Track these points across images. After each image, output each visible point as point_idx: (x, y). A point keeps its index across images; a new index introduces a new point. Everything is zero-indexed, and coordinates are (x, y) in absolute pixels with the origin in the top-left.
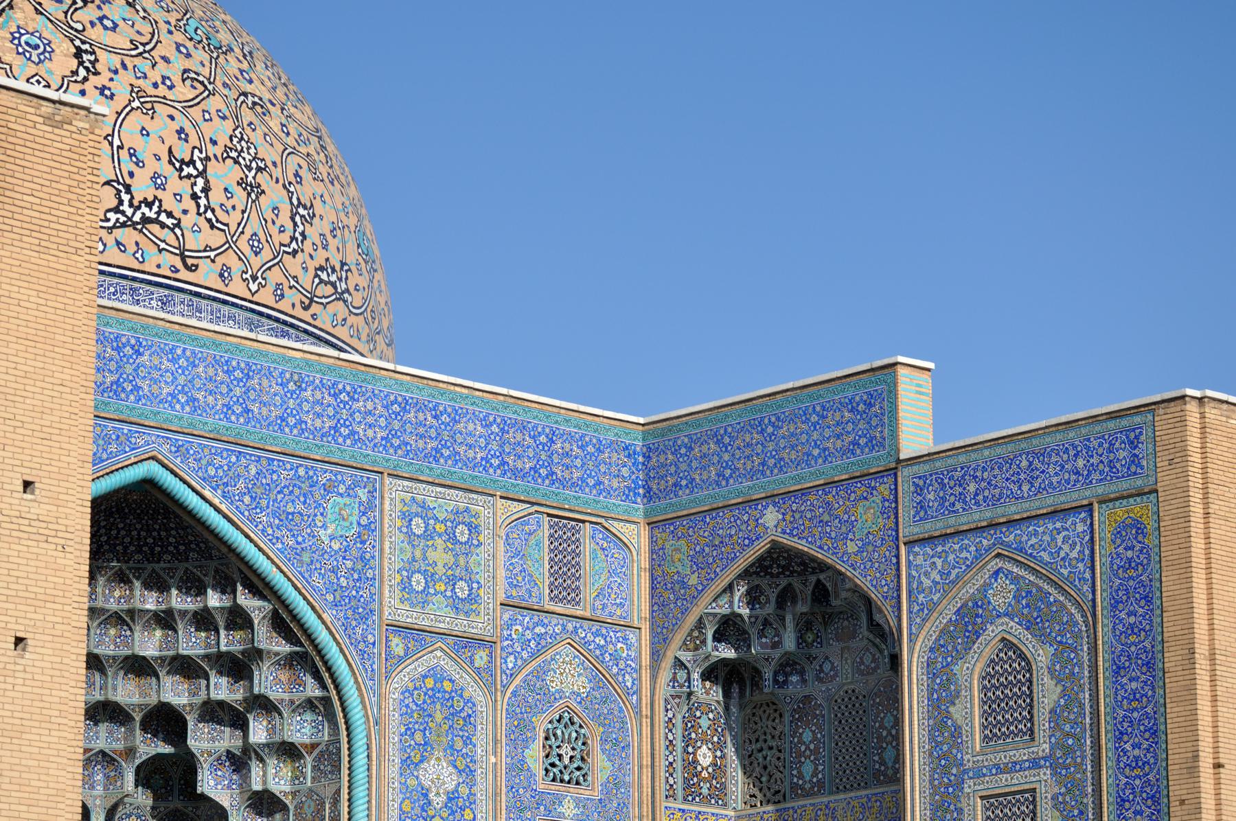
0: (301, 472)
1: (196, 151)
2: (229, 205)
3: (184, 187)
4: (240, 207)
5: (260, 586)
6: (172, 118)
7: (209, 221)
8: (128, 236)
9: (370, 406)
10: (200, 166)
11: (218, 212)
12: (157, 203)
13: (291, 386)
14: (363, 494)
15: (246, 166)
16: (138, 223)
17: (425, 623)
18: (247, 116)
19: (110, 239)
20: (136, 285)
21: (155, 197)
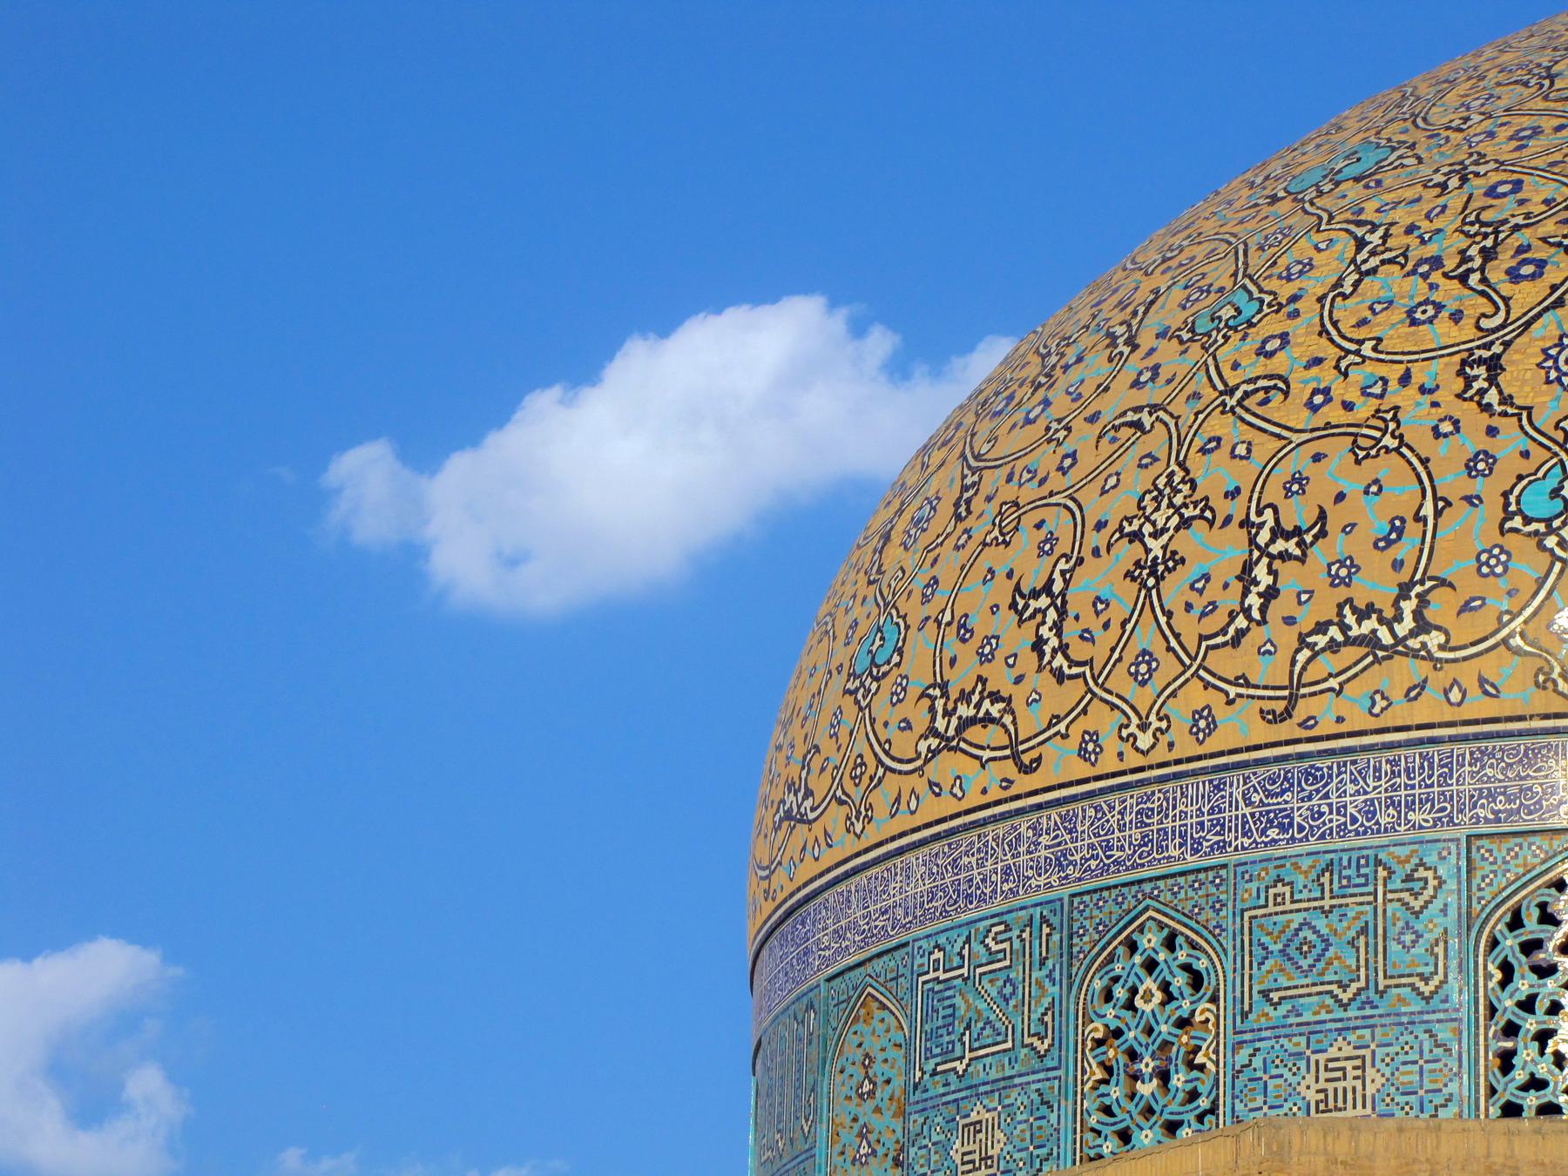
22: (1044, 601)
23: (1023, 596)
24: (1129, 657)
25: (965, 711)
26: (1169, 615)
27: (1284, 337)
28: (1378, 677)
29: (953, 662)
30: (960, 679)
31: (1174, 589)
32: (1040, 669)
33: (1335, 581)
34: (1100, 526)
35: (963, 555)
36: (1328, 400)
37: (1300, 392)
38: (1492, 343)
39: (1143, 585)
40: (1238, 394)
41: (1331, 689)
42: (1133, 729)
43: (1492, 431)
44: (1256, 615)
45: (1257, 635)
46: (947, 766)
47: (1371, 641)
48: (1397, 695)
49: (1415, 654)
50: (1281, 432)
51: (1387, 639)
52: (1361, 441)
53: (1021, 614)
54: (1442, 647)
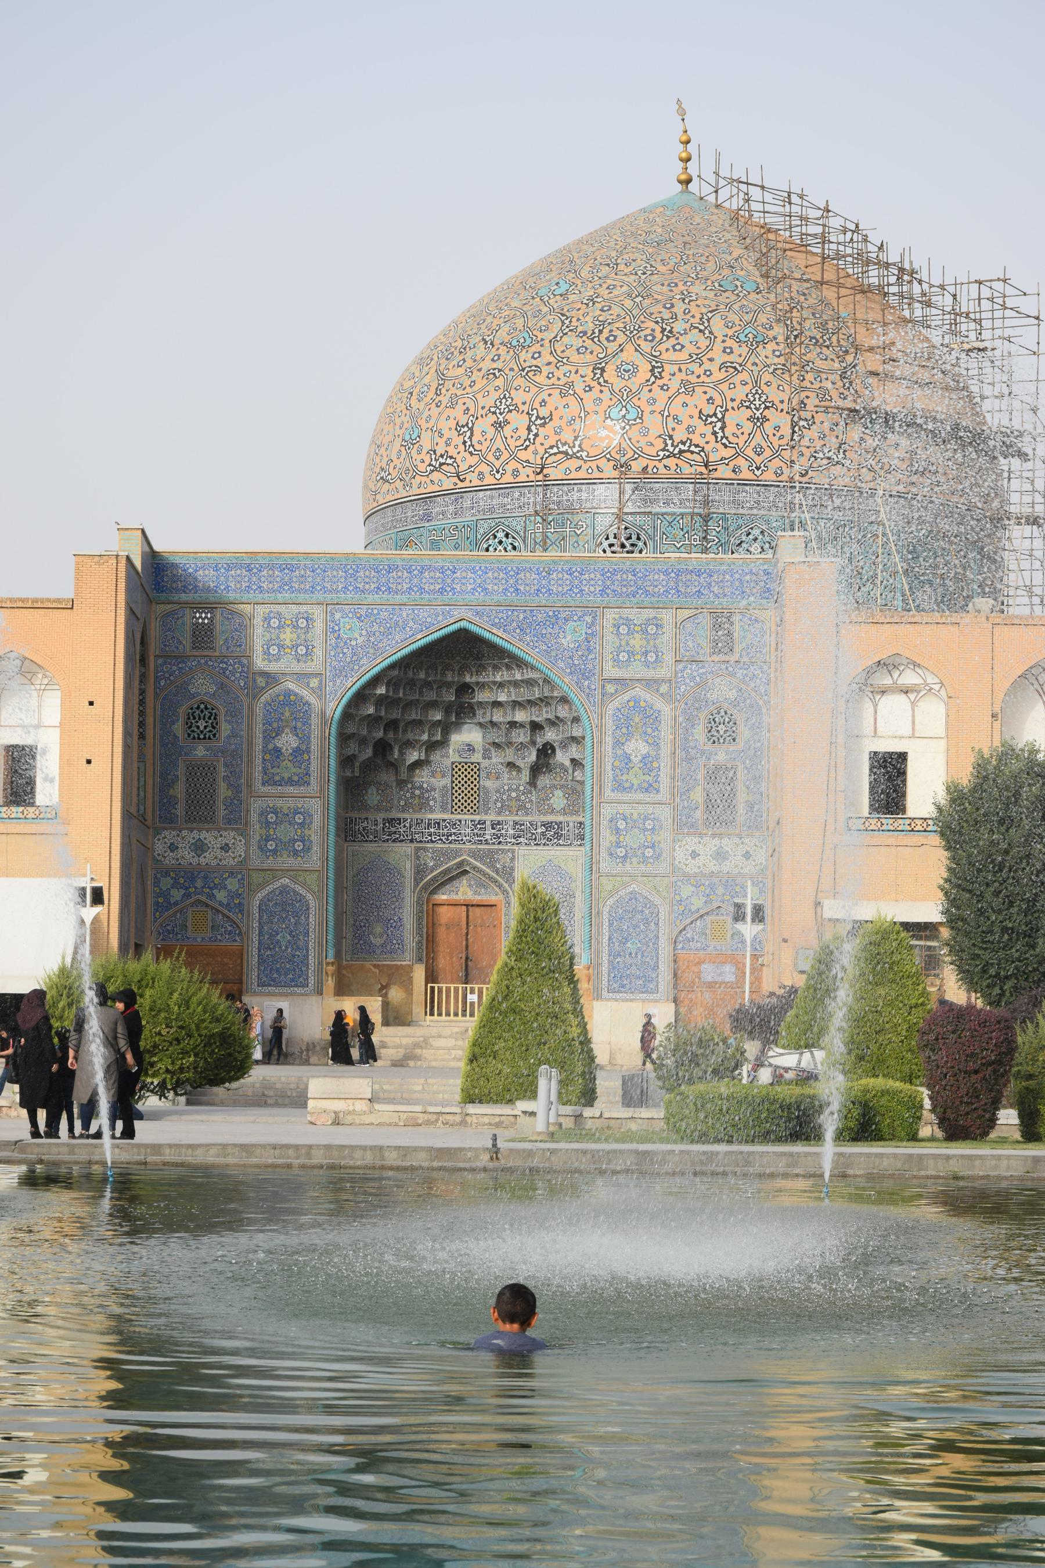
0: (551, 613)
2: (739, 433)
4: (747, 431)
5: (533, 668)
6: (705, 393)
7: (724, 444)
8: (671, 462)
9: (592, 576)
10: (720, 416)
11: (732, 439)
13: (544, 574)
14: (589, 619)
17: (628, 676)
18: (766, 377)
19: (660, 466)
20: (678, 485)
22: (466, 429)
25: (442, 460)
27: (539, 353)
31: (508, 431)
33: (556, 433)
34: (483, 408)
35: (439, 410)
37: (545, 373)
43: (601, 391)
45: (532, 448)
46: (436, 476)
47: (566, 453)
49: (578, 458)
50: (539, 386)
51: (570, 453)
54: (587, 456)
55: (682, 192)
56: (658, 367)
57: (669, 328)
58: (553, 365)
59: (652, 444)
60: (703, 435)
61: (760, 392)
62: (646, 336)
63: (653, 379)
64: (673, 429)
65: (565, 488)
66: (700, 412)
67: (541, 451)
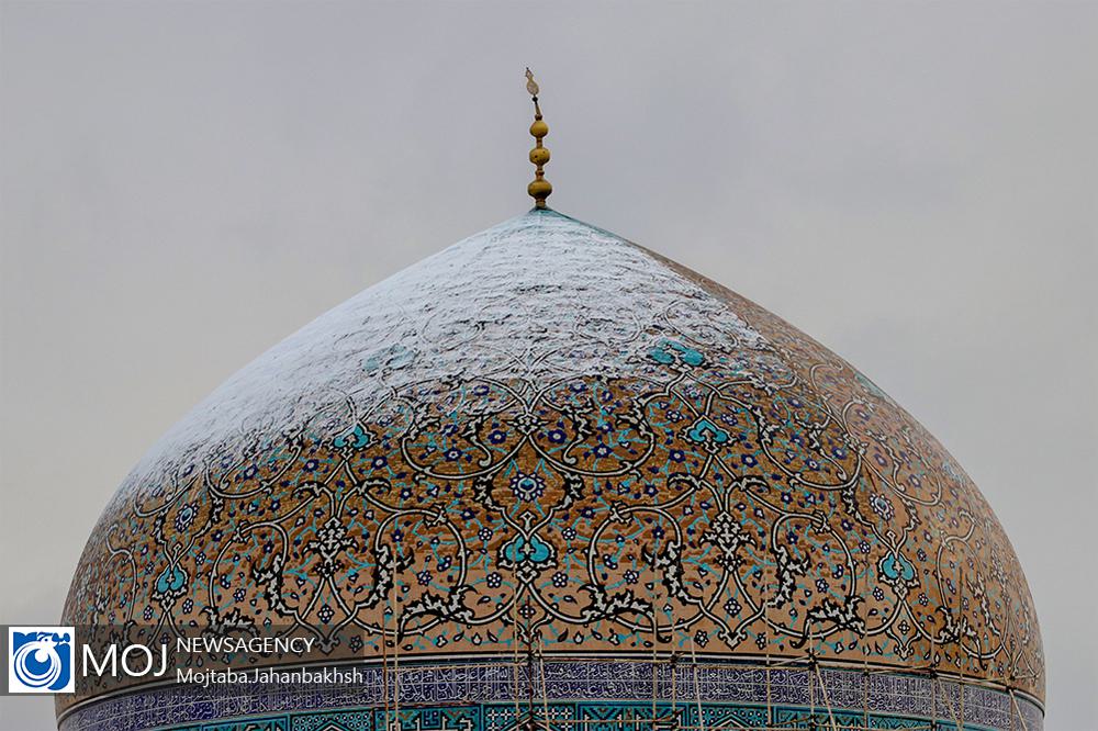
1: (671, 543)
2: (703, 583)
3: (657, 576)
7: (682, 599)
8: (603, 627)
10: (673, 555)
11: (692, 590)
12: (629, 595)
15: (726, 545)
16: (611, 615)
21: (627, 590)
22: (269, 575)
23: (257, 571)
24: (317, 609)
26: (339, 590)
28: (439, 630)
29: (219, 598)
30: (226, 606)
32: (270, 609)
36: (411, 495)
38: (487, 474)
39: (322, 576)
40: (364, 487)
41: (419, 633)
42: (320, 642)
44: (382, 595)
47: (438, 613)
48: (450, 640)
49: (457, 620)
51: (444, 609)
52: (428, 518)
53: (257, 580)
54: (471, 618)
55: (538, 208)
56: (575, 482)
57: (584, 422)
58: (409, 477)
59: (573, 600)
60: (650, 586)
61: (729, 519)
62: (551, 433)
63: (568, 500)
64: (605, 576)
65: (437, 667)
66: (644, 550)
67: (397, 609)
